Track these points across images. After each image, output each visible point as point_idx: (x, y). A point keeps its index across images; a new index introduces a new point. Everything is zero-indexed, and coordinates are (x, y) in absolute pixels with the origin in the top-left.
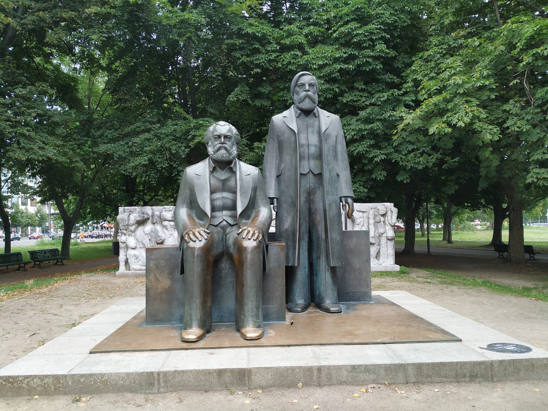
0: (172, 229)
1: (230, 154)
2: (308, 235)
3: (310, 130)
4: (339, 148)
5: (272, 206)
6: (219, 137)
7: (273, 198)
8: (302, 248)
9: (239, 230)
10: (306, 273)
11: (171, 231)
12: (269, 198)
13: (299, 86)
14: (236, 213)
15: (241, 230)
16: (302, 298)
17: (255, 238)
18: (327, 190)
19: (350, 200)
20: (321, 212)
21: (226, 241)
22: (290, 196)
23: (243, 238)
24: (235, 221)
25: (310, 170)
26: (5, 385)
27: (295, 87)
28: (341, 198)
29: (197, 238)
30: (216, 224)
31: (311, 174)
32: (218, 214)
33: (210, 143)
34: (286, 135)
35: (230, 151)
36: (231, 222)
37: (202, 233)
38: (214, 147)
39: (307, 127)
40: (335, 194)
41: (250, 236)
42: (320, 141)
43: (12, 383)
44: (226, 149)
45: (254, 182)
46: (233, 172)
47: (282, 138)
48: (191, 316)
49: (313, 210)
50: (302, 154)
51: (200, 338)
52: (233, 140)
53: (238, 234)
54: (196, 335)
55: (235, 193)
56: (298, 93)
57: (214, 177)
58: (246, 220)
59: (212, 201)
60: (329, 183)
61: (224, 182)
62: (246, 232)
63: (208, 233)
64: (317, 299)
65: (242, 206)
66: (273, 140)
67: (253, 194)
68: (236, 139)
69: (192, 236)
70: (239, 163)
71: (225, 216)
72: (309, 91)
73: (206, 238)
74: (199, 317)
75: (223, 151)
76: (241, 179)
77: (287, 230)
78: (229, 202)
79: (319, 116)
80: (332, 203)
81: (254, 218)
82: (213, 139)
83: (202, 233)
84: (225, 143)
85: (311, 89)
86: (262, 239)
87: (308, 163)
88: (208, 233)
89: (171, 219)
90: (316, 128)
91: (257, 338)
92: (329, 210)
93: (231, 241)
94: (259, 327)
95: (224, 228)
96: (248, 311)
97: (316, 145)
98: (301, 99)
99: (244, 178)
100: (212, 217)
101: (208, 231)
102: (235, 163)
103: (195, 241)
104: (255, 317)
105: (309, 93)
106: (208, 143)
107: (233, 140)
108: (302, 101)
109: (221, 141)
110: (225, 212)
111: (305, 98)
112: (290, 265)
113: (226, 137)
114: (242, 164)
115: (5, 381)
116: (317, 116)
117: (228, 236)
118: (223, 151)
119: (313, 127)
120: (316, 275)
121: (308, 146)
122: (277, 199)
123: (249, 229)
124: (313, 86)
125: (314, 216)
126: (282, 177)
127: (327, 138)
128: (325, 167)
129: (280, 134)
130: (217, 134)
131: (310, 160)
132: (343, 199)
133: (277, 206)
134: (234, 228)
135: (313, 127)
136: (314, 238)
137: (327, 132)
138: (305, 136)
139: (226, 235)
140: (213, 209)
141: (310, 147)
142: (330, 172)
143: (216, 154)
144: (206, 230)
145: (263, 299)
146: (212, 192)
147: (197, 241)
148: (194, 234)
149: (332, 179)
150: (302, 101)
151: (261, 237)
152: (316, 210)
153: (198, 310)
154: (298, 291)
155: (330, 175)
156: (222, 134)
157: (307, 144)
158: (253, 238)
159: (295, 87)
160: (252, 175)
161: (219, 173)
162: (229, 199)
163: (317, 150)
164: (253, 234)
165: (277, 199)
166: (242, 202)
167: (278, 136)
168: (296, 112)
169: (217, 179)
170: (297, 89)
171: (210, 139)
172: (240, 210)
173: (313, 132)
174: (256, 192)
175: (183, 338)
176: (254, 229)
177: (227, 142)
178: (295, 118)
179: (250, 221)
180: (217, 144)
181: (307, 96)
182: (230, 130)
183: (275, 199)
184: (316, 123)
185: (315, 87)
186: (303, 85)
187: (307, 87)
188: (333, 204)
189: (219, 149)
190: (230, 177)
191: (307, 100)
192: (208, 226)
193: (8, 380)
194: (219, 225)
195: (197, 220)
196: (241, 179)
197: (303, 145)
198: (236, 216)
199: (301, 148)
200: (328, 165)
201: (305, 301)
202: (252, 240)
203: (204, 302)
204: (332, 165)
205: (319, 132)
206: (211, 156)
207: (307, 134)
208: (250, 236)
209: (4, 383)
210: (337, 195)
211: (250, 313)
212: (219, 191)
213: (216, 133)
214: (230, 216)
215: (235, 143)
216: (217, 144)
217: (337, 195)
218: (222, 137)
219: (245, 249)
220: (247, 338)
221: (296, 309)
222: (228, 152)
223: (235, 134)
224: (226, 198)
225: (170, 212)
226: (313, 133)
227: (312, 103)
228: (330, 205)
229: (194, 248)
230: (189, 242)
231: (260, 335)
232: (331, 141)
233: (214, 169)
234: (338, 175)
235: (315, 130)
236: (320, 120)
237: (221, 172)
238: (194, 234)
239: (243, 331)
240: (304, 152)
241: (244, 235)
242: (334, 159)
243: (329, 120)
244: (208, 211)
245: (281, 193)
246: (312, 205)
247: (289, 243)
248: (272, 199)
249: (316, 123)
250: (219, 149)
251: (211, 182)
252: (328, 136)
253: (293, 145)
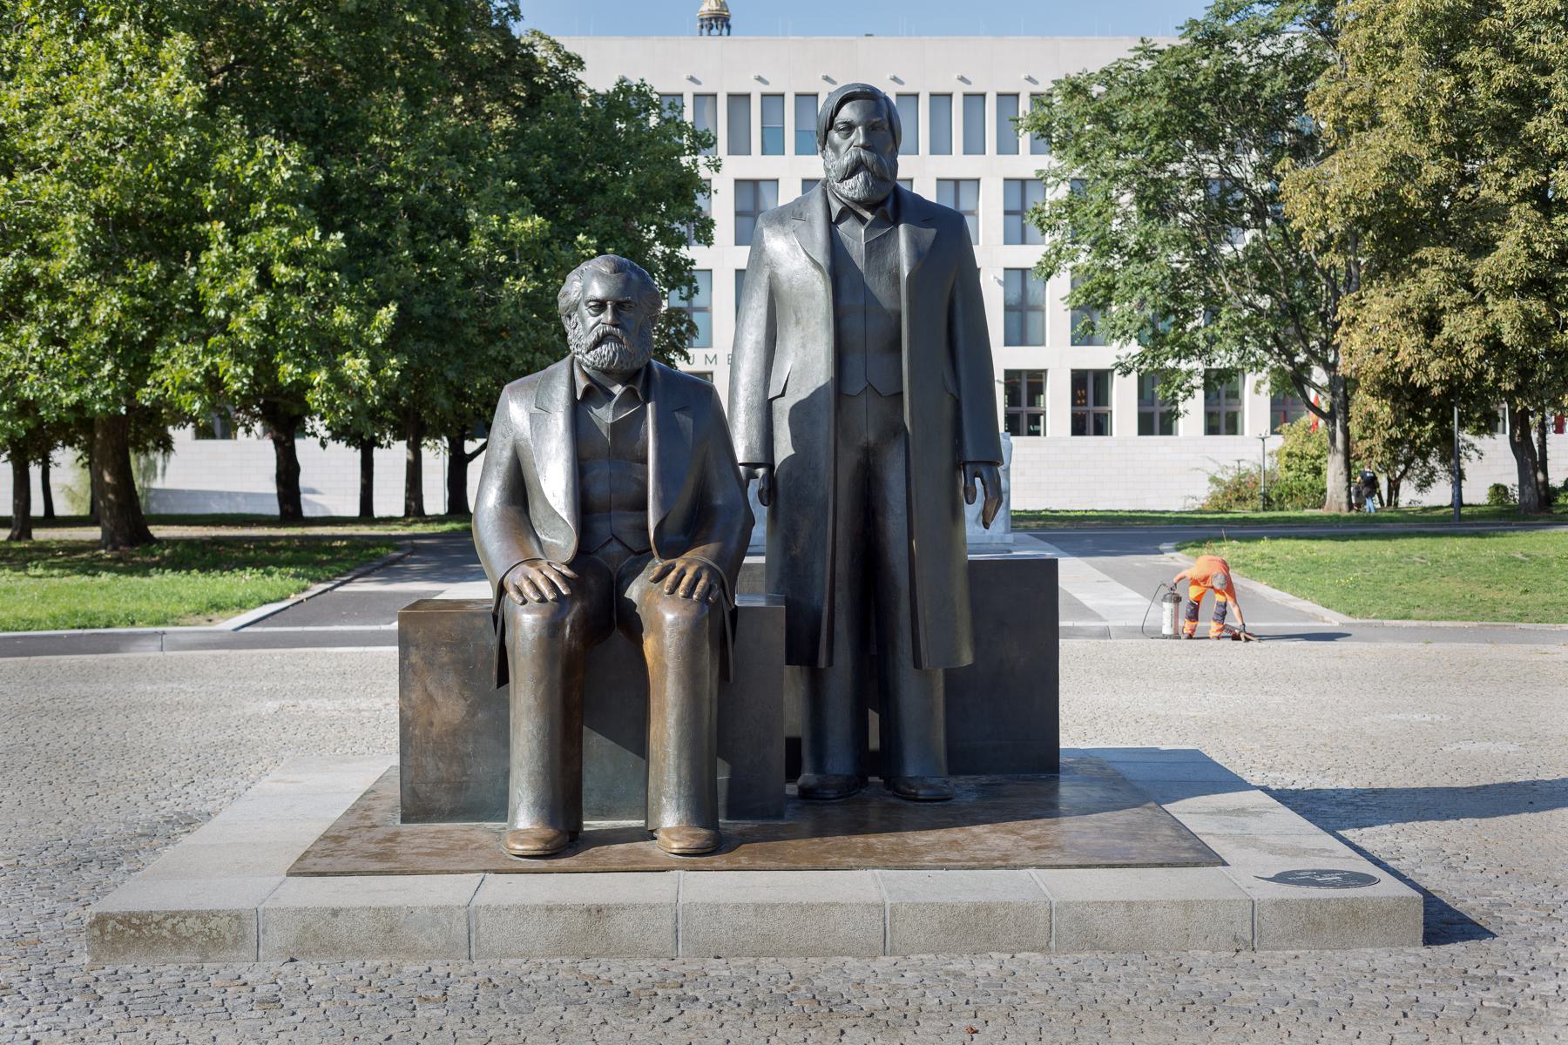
26: (123, 931)
43: (138, 928)
62: (673, 574)
115: (121, 922)
148: (533, 584)
186: (849, 127)
193: (129, 921)
198: (646, 529)
209: (120, 927)
238: (533, 584)
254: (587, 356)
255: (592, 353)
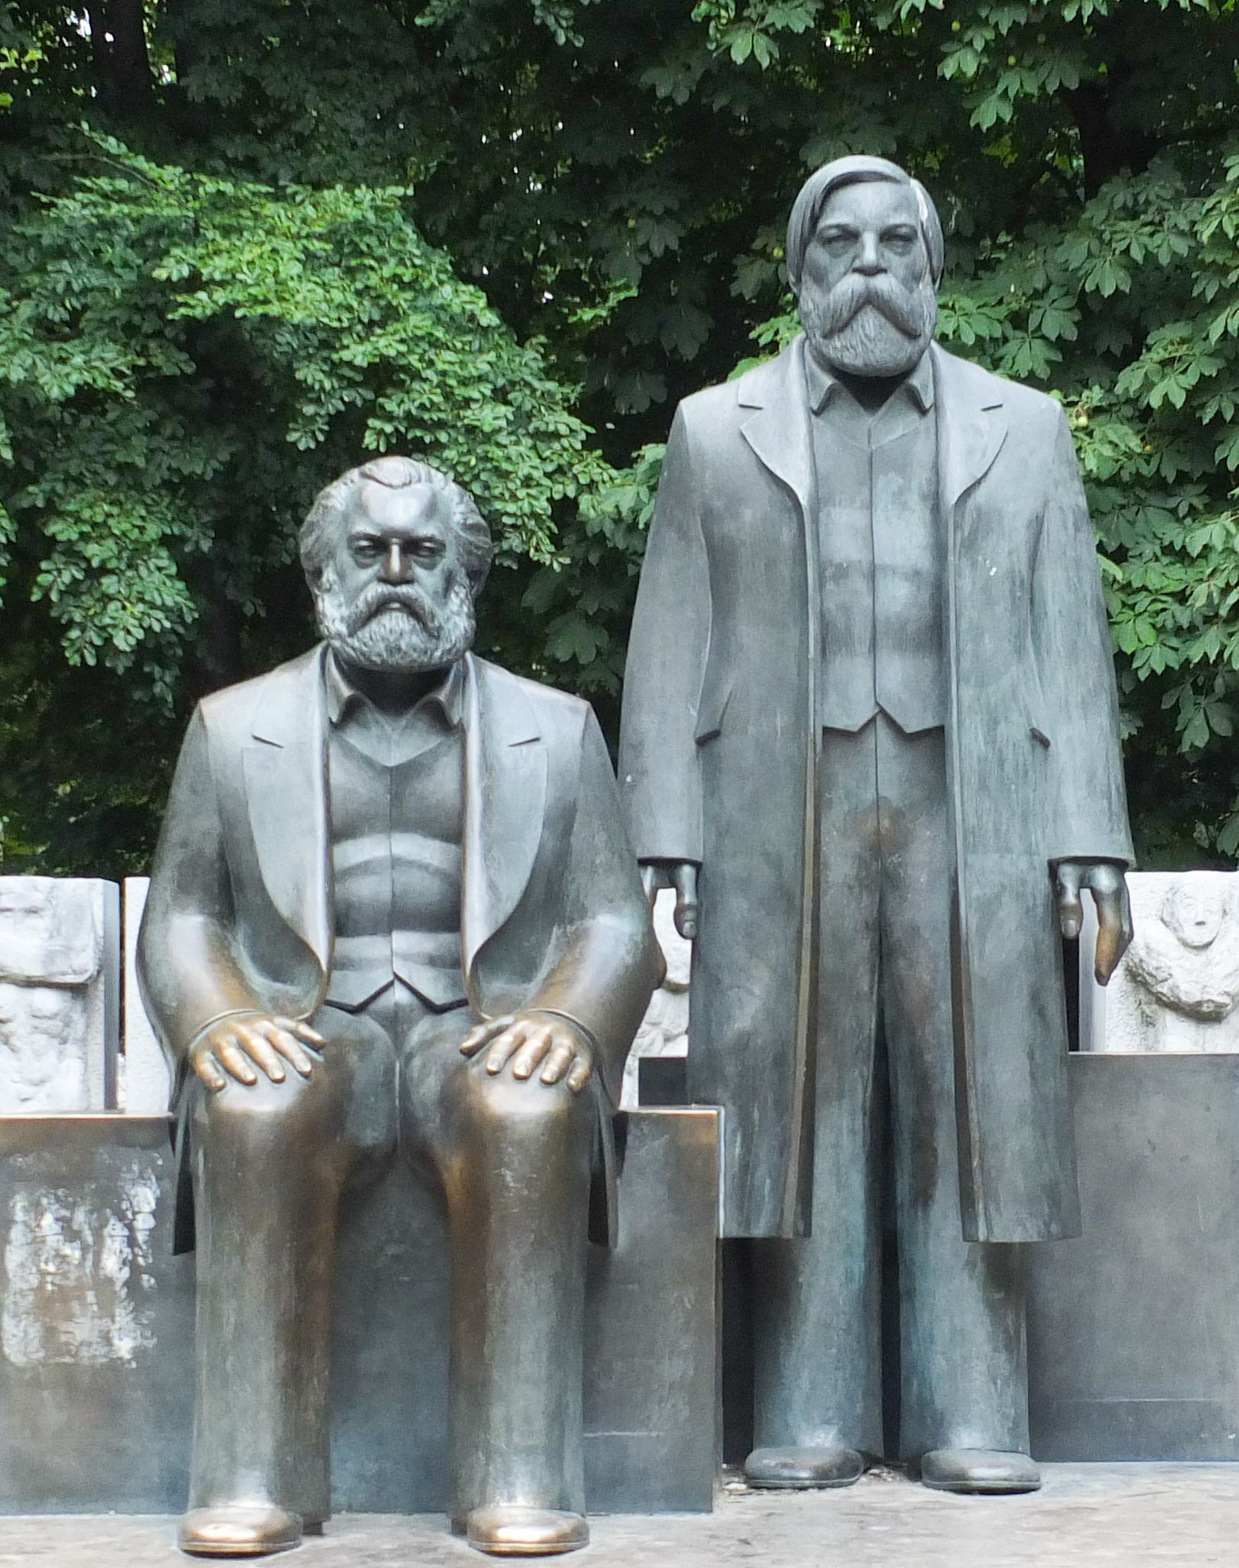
0: (41, 1039)
1: (434, 634)
2: (868, 1070)
3: (887, 483)
4: (1054, 583)
5: (666, 900)
6: (379, 545)
7: (677, 863)
8: (836, 1146)
9: (469, 1033)
10: (855, 1286)
11: (38, 1055)
12: (644, 863)
13: (828, 241)
14: (461, 944)
15: (479, 1033)
16: (827, 1422)
17: (549, 1071)
18: (972, 821)
19: (1104, 878)
20: (940, 943)
21: (405, 1093)
22: (767, 855)
23: (492, 1074)
24: (455, 984)
25: (882, 711)
27: (804, 244)
28: (1053, 868)
29: (262, 1067)
30: (357, 1000)
31: (882, 731)
32: (362, 946)
33: (329, 575)
34: (748, 514)
35: (433, 617)
36: (437, 994)
37: (285, 1040)
38: (352, 597)
39: (871, 466)
40: (1017, 844)
41: (522, 1063)
42: (940, 551)
44: (410, 608)
45: (558, 776)
46: (444, 722)
47: (729, 527)
48: (229, 1441)
49: (898, 934)
50: (840, 621)
51: (273, 1542)
52: (450, 559)
53: (469, 1053)
54: (254, 1527)
55: (455, 835)
56: (821, 279)
57: (349, 751)
58: (510, 981)
59: (334, 876)
60: (983, 786)
61: (401, 776)
62: (505, 1041)
63: (315, 1046)
64: (910, 1432)
65: (493, 906)
66: (684, 535)
67: (550, 844)
68: (468, 549)
69: (233, 1055)
70: (479, 676)
71: (406, 957)
72: (884, 271)
73: (307, 1067)
74: (266, 1445)
75: (396, 622)
76: (488, 767)
77: (743, 1043)
78: (426, 889)
79: (936, 406)
80: (998, 897)
81: (553, 972)
82: (345, 557)
83: (285, 1040)
84: (409, 575)
85: (895, 261)
86: (587, 1079)
87: (868, 671)
88: (316, 1047)
89: (36, 971)
90: (921, 477)
91: (544, 1547)
92: (982, 933)
93: (429, 1087)
94: (562, 1504)
95: (395, 1022)
96: (509, 1430)
97: (917, 573)
98: (835, 316)
99: (507, 757)
100: (335, 964)
101: (316, 1036)
102: (464, 677)
103: (251, 1084)
104: (542, 1459)
105: (883, 284)
106: (319, 573)
107: (450, 559)
108: (839, 324)
109: (387, 565)
110: (404, 941)
111: (856, 312)
112: (760, 1230)
113: (412, 546)
114: (497, 676)
116: (928, 403)
117: (417, 1062)
118: (396, 622)
119: (902, 468)
120: (911, 1293)
121: (872, 574)
122: (697, 866)
123: (523, 1025)
124: (908, 239)
125: (902, 963)
126: (726, 745)
127: (974, 531)
128: (964, 694)
129: (718, 504)
130: (371, 530)
131: (883, 654)
132: (1069, 876)
133: (697, 908)
134: (451, 1021)
135: (902, 468)
136: (904, 1093)
137: (980, 496)
138: (857, 517)
139: (410, 1057)
140: (342, 924)
141: (881, 583)
142: (993, 724)
143: (364, 634)
144: (305, 1030)
145: (589, 1389)
146: (336, 834)
147: (263, 1081)
148: (244, 1047)
149: (1001, 763)
150: (839, 324)
151: (581, 1068)
152: (914, 931)
153: (263, 1415)
154: (804, 1382)
155: (991, 741)
156: (395, 533)
157: (865, 566)
158: (538, 1072)
159: (804, 244)
160: (549, 740)
161: (374, 730)
162: (425, 867)
163: (925, 597)
164: (546, 1050)
165: (697, 866)
166: (492, 886)
167: (709, 517)
168: (809, 380)
169: (368, 762)
170: (817, 253)
171: (331, 555)
172: (476, 933)
173: (899, 496)
174: (567, 831)
175: (197, 1538)
176: (547, 1030)
177: (419, 572)
178: (800, 416)
179: (533, 987)
180: (366, 584)
181: (870, 300)
182: (432, 510)
183: (687, 872)
184: (922, 450)
185: (920, 245)
186: (850, 235)
187: (870, 252)
188: (1005, 899)
189: (380, 607)
190: (434, 754)
191: (870, 322)
192: (317, 1010)
194: (373, 1007)
195: (258, 981)
196: (488, 767)
197: (842, 572)
198: (457, 963)
199: (830, 586)
200: (982, 684)
201: (844, 1434)
202: (534, 1082)
203: (293, 1381)
204: (1005, 682)
205: (935, 499)
206: (337, 643)
207: (870, 506)
208: (522, 1063)
210: (1030, 852)
211: (516, 1438)
212: (373, 830)
213: (362, 527)
214: (433, 961)
215: (461, 576)
216: (366, 584)
217: (1030, 852)
218: (395, 550)
219: (499, 1126)
220: (498, 1548)
221: (786, 1473)
222: (425, 627)
223: (467, 527)
224: (410, 864)
225: (33, 921)
226: (904, 506)
227: (894, 334)
228: (988, 908)
229: (248, 1117)
230: (221, 1088)
231: (562, 1538)
232: (1005, 547)
233: (349, 714)
234: (1040, 741)
235: (914, 484)
236: (942, 430)
237: (388, 729)
238: (244, 1047)
239: (479, 1518)
240: (845, 609)
241: (494, 1058)
242: (1019, 651)
243: (993, 427)
244: (317, 935)
245: (720, 835)
246: (892, 900)
247: (756, 1115)
248: (667, 869)
249: (922, 450)
250: (380, 607)
251: (337, 776)
252: (985, 523)
253: (785, 570)
254: (349, 640)
255: (360, 634)
